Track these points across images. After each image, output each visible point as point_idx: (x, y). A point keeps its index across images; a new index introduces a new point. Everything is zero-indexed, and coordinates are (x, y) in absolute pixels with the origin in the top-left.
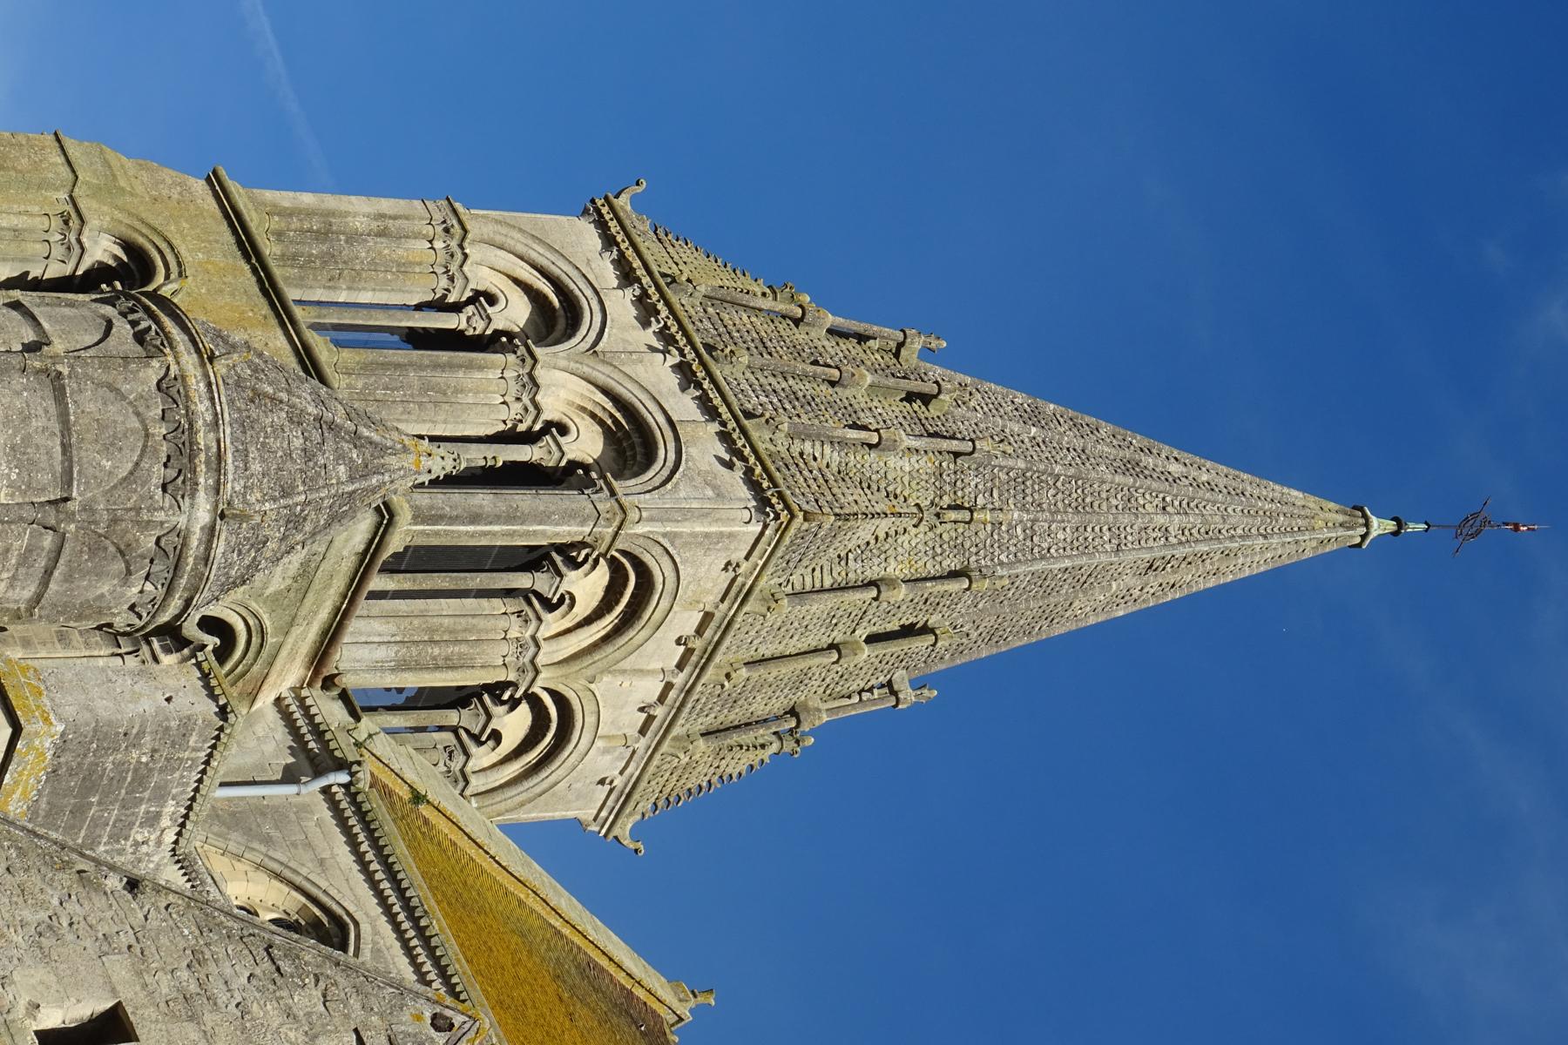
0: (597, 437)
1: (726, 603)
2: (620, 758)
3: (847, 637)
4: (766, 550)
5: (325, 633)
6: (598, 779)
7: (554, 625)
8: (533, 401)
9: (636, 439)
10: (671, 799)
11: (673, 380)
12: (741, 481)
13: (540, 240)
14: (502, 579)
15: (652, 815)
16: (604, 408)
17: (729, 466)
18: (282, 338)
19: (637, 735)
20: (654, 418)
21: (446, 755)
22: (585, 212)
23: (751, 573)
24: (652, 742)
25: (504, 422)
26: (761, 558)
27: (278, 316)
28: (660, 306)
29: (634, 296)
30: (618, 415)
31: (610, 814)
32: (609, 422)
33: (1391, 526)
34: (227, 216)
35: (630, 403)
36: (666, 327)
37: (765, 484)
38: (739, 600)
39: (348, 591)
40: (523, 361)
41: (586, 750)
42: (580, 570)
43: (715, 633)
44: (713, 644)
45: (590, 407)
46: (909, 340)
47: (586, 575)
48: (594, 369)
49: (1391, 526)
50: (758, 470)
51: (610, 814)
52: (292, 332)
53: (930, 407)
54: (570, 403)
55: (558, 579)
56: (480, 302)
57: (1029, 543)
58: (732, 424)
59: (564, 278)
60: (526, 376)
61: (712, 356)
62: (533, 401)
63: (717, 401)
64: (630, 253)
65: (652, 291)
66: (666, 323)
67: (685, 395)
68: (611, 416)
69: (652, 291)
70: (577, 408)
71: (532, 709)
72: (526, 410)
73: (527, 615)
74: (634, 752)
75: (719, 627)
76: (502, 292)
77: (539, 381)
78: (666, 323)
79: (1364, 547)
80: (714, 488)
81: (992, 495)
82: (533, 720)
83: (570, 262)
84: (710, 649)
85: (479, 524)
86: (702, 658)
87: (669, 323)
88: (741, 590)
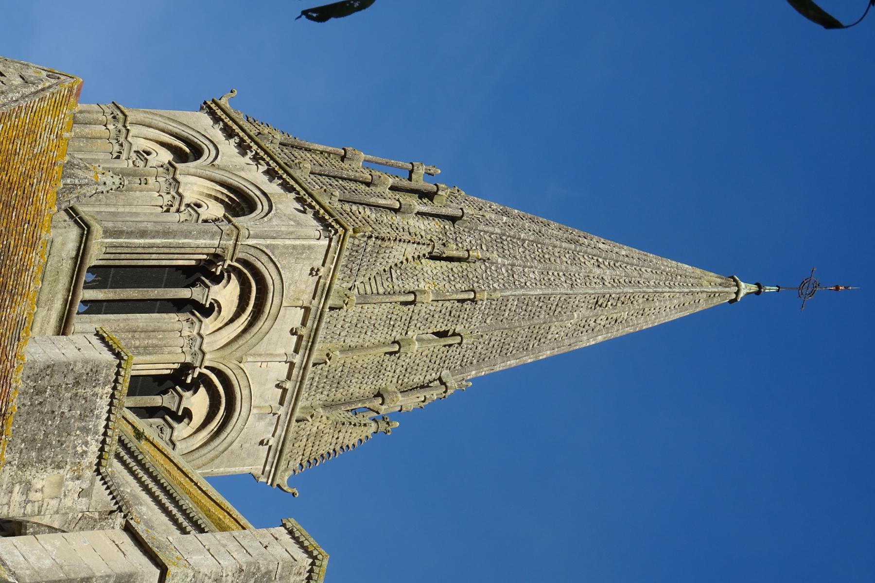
0: (220, 209)
1: (317, 298)
2: (270, 424)
3: (404, 337)
4: (334, 257)
5: (61, 319)
6: (259, 441)
7: (211, 326)
8: (177, 193)
10: (311, 461)
11: (265, 178)
14: (171, 291)
15: (300, 472)
16: (222, 193)
17: (304, 212)
19: (278, 406)
21: (159, 430)
22: (202, 108)
23: (328, 275)
24: (288, 410)
25: (161, 207)
26: (332, 264)
28: (252, 144)
29: (236, 143)
30: (231, 195)
31: (272, 467)
32: (227, 200)
33: (754, 288)
36: (257, 153)
37: (327, 217)
38: (324, 296)
39: (71, 286)
40: (168, 170)
41: (247, 416)
42: (220, 284)
43: (314, 322)
44: (314, 331)
45: (213, 193)
46: (415, 168)
47: (225, 287)
49: (754, 288)
50: (322, 211)
51: (272, 467)
53: (434, 201)
54: (201, 194)
55: (207, 289)
57: (511, 278)
62: (177, 193)
63: (292, 182)
64: (230, 123)
65: (246, 138)
67: (272, 184)
68: (227, 196)
69: (246, 138)
70: (206, 196)
71: (208, 391)
72: (174, 197)
73: (192, 320)
74: (279, 417)
75: (315, 318)
77: (179, 180)
79: (739, 300)
80: (295, 221)
81: (482, 248)
82: (210, 401)
84: (312, 334)
85: (146, 238)
86: (308, 342)
87: (258, 151)
88: (323, 290)
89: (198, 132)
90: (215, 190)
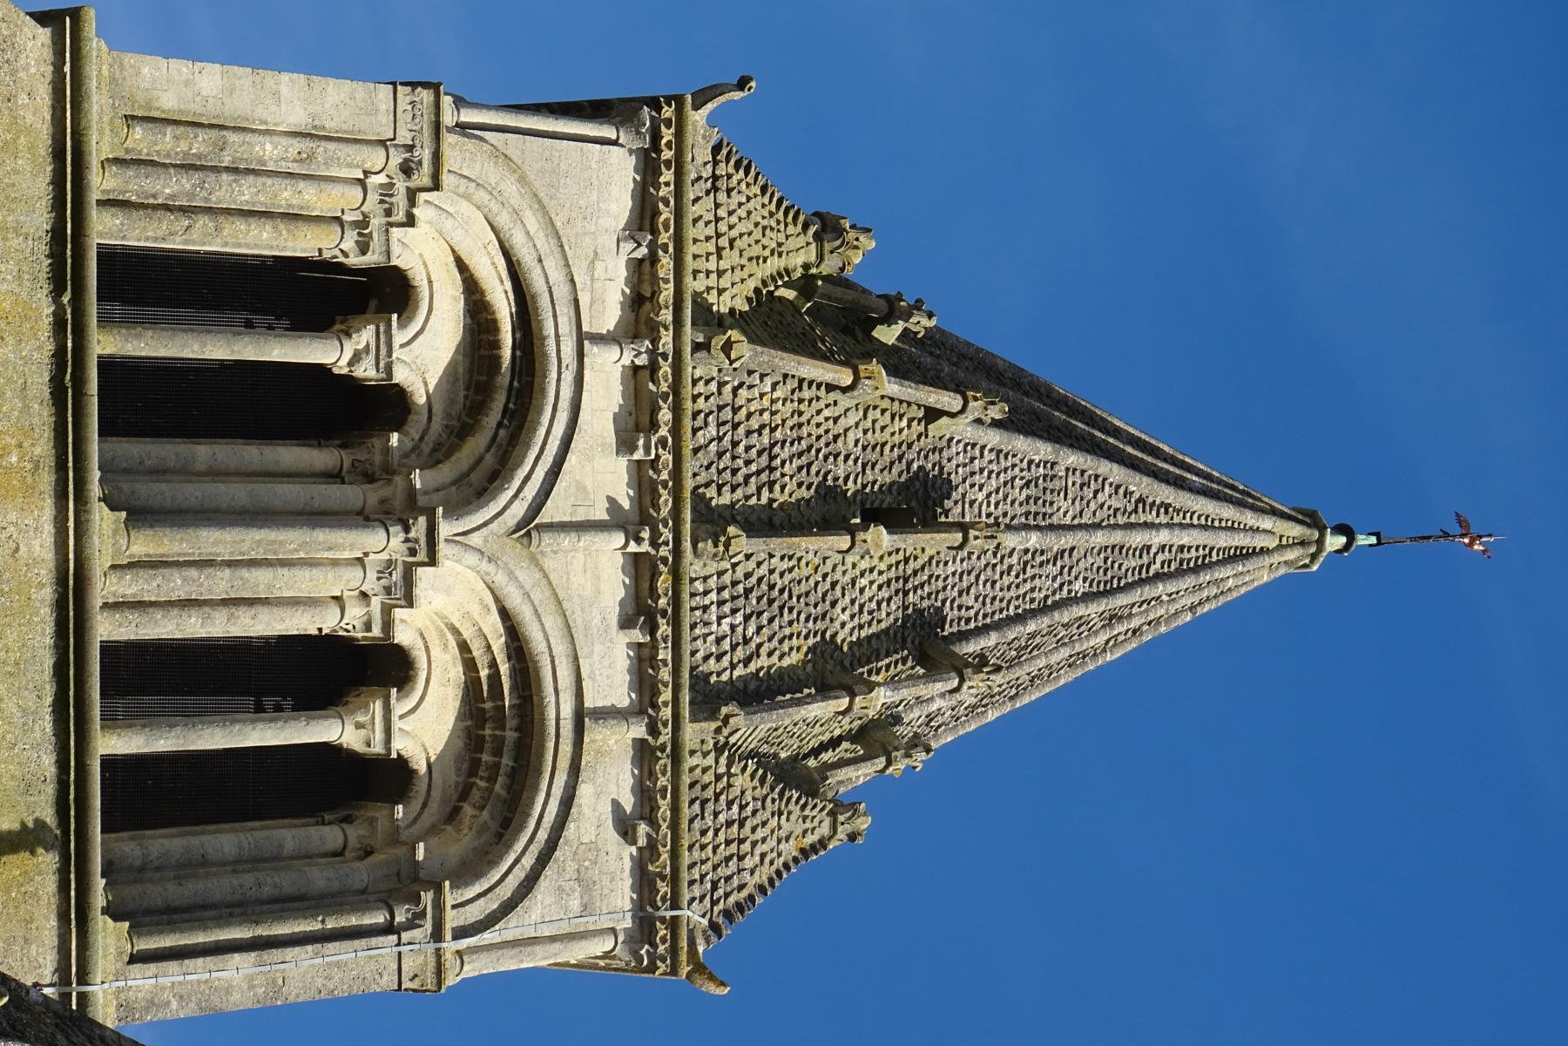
9: (511, 735)
11: (613, 586)
12: (628, 864)
13: (542, 207)
16: (489, 647)
17: (625, 829)
18: (48, 529)
20: (558, 708)
27: (61, 466)
29: (633, 362)
30: (501, 658)
34: (58, 154)
35: (536, 662)
36: (654, 464)
37: (663, 888)
45: (467, 634)
48: (511, 575)
49: (1342, 540)
52: (71, 524)
56: (390, 320)
58: (666, 736)
59: (544, 302)
60: (400, 569)
62: (387, 611)
64: (666, 263)
66: (658, 457)
68: (493, 665)
69: (665, 368)
70: (446, 624)
76: (430, 282)
78: (658, 457)
83: (567, 265)
89: (572, 280)
90: (480, 629)
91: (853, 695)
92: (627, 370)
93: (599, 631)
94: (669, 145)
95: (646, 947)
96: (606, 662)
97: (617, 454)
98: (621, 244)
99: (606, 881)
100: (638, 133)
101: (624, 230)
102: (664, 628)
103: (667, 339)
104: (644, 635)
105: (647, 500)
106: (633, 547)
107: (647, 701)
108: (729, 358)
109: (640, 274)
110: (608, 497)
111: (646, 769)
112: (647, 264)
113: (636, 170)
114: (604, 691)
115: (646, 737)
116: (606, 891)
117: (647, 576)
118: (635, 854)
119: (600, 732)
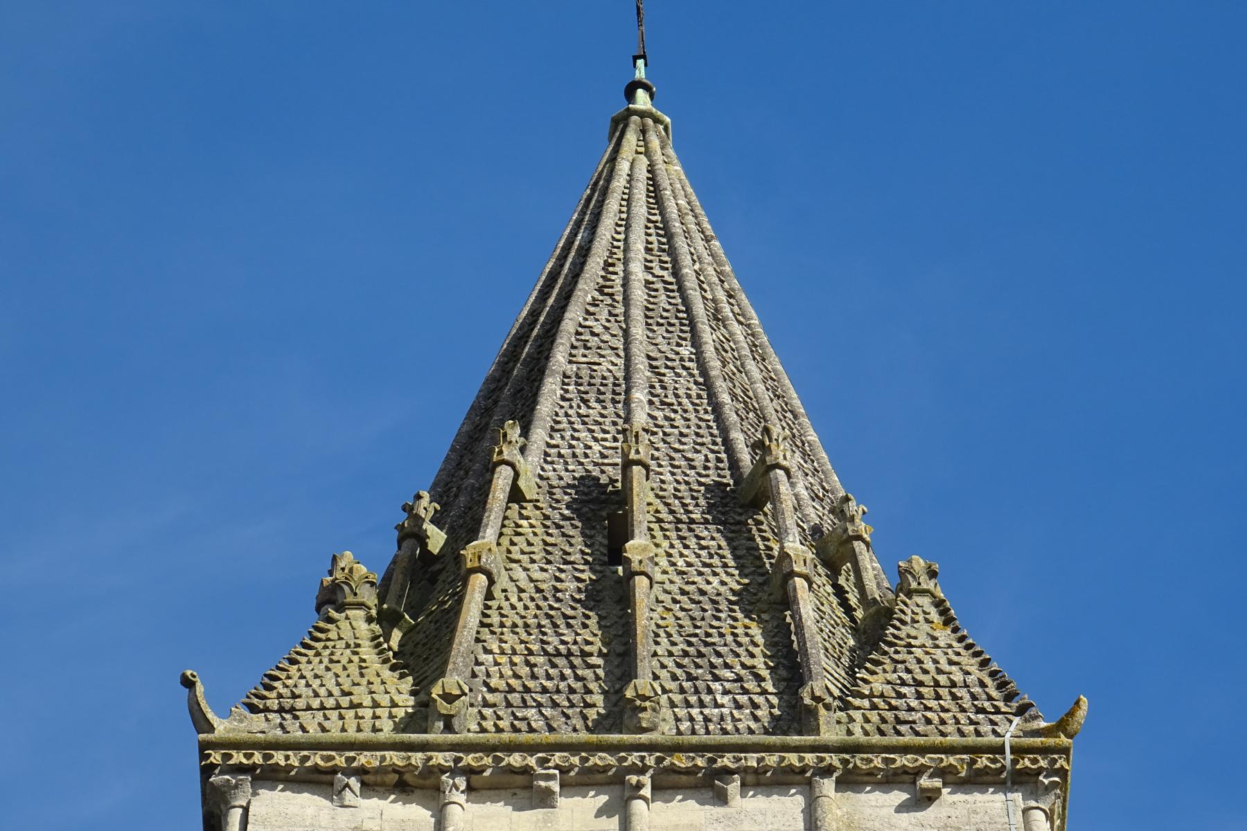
12: (959, 797)
17: (925, 799)
29: (462, 792)
36: (564, 771)
37: (983, 761)
49: (641, 93)
58: (833, 759)
61: (645, 730)
64: (365, 759)
66: (557, 767)
67: (732, 803)
69: (469, 759)
78: (557, 767)
91: (792, 574)
92: (470, 798)
93: (729, 826)
94: (248, 756)
95: (1041, 778)
96: (760, 818)
97: (554, 807)
98: (347, 803)
99: (976, 819)
100: (236, 787)
101: (332, 801)
102: (727, 761)
103: (440, 758)
104: (733, 781)
105: (599, 777)
106: (646, 792)
107: (798, 778)
108: (460, 696)
109: (376, 784)
110: (597, 816)
111: (866, 778)
112: (366, 778)
113: (273, 789)
114: (788, 820)
115: (834, 778)
116: (987, 818)
117: (676, 777)
118: (949, 790)
119: (829, 824)
